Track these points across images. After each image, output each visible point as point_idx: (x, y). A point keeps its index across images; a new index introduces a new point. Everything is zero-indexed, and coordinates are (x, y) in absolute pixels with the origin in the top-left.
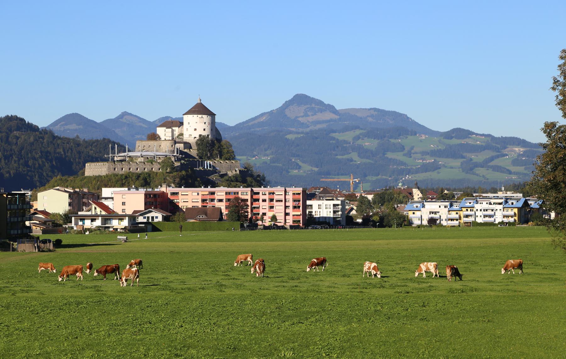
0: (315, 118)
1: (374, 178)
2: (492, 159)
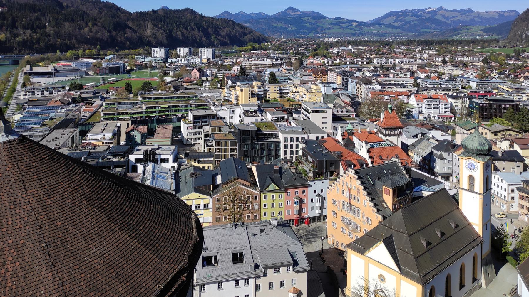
0: (295, 13)
2: (349, 26)
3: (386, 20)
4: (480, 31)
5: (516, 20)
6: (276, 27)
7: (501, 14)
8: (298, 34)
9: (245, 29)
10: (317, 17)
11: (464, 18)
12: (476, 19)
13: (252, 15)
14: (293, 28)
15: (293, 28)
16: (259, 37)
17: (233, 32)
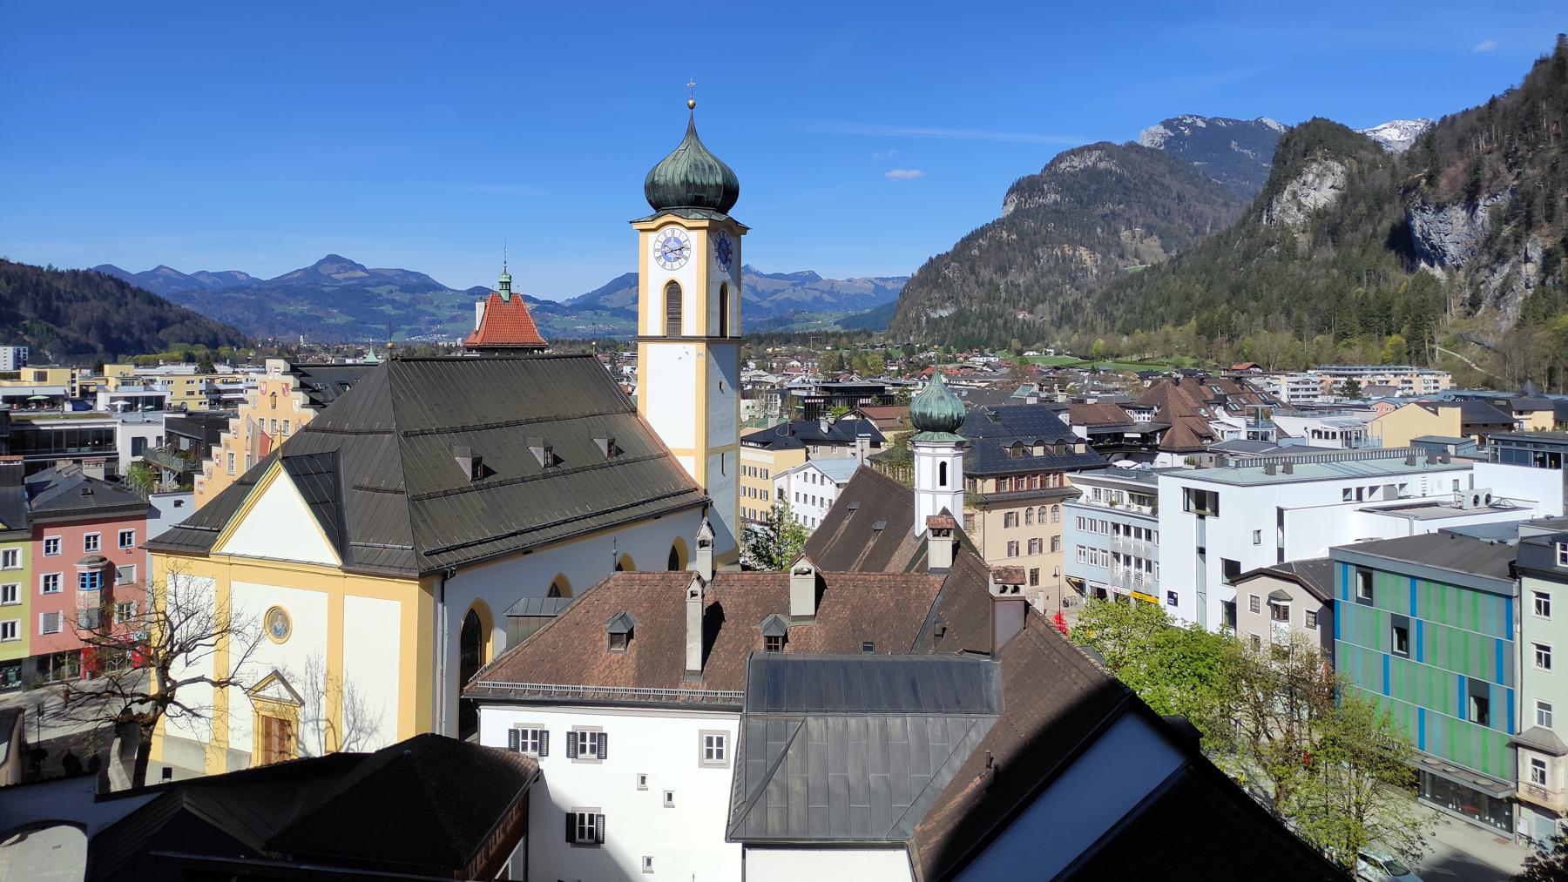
0: (347, 275)
1: (409, 327)
3: (613, 296)
4: (835, 324)
5: (907, 286)
6: (285, 315)
7: (879, 285)
8: (356, 336)
9: (166, 307)
10: (422, 286)
11: (800, 295)
12: (827, 298)
13: (202, 278)
14: (342, 319)
15: (342, 319)
16: (216, 335)
17: (117, 318)
